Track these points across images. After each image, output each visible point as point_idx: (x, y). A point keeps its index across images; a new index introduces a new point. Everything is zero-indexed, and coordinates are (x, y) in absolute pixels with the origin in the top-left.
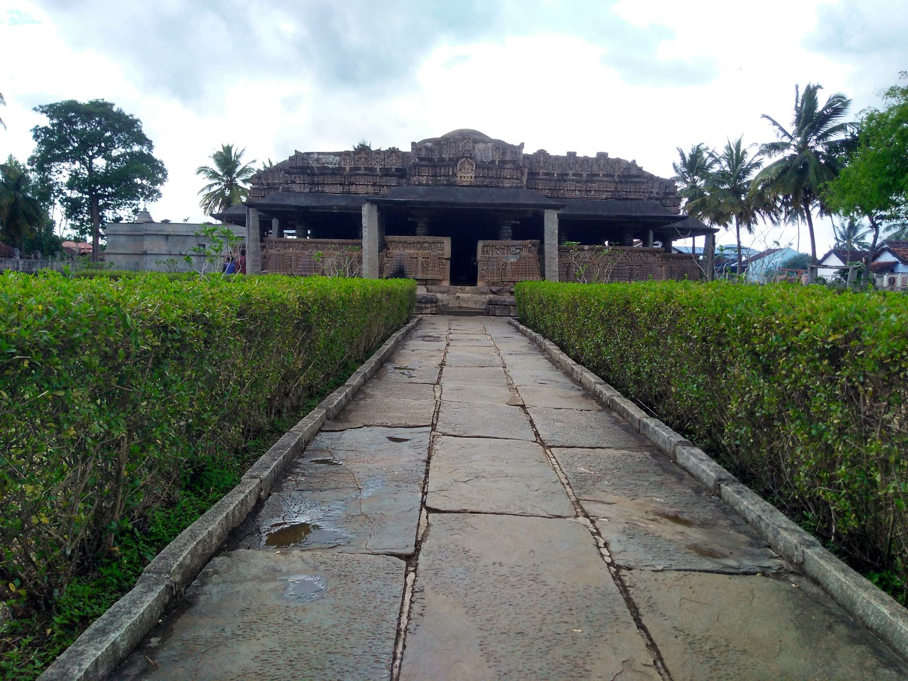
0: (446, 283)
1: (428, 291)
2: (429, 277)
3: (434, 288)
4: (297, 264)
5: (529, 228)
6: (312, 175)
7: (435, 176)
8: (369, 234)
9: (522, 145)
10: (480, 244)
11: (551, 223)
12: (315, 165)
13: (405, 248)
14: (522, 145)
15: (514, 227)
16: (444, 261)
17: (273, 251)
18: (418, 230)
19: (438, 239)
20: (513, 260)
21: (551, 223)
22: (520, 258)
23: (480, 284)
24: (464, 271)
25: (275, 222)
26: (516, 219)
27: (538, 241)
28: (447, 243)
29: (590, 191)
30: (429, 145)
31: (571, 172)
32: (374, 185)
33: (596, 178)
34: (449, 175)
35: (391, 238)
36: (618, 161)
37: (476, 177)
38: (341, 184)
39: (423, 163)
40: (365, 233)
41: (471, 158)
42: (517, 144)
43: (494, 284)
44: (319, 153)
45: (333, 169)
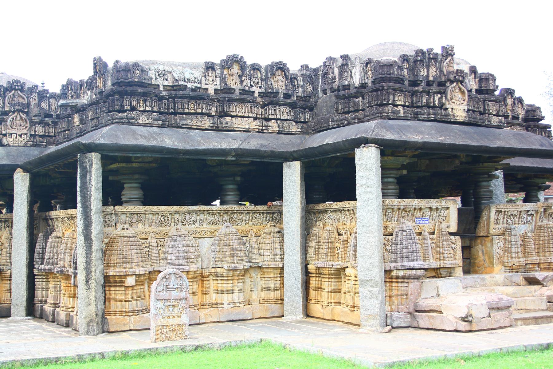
12: (161, 82)
34: (434, 107)
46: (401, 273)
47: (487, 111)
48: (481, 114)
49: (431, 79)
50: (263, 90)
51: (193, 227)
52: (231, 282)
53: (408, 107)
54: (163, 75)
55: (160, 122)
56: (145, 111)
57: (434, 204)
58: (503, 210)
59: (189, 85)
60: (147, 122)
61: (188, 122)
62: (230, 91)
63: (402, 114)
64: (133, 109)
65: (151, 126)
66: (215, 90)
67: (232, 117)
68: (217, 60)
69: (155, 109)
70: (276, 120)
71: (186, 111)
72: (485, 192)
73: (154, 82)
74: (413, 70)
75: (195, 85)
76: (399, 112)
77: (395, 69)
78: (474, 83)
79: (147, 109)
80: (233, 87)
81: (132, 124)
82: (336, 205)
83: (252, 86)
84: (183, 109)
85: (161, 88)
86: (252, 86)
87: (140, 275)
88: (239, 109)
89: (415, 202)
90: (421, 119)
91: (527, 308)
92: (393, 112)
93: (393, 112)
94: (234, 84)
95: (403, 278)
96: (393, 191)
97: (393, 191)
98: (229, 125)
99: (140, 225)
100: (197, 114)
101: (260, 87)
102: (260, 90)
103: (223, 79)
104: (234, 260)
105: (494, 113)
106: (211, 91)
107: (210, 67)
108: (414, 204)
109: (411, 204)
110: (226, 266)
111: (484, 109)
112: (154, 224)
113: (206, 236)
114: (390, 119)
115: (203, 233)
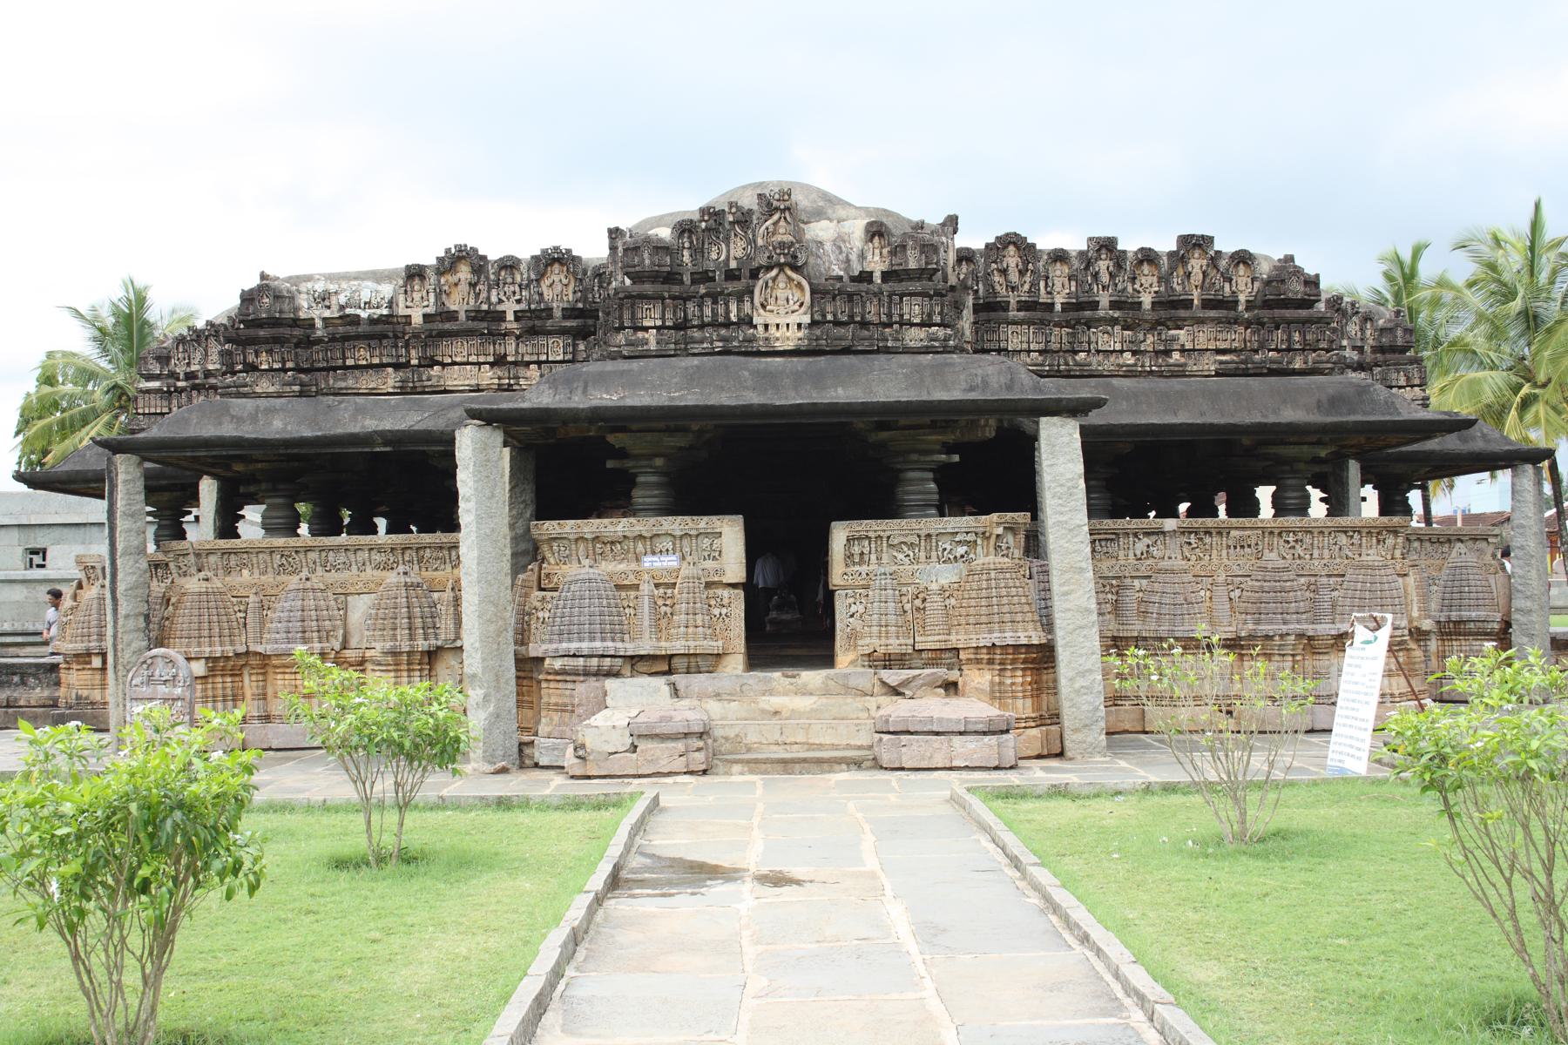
0: (736, 663)
1: (675, 692)
2: (678, 646)
3: (698, 681)
4: (262, 623)
5: (987, 471)
6: (308, 342)
7: (682, 326)
8: (479, 518)
9: (952, 223)
10: (840, 534)
11: (1060, 456)
12: (318, 314)
13: (597, 557)
14: (952, 223)
15: (943, 475)
17: (193, 584)
18: (639, 496)
19: (703, 522)
21: (1060, 456)
22: (971, 573)
23: (844, 658)
24: (788, 621)
25: (208, 489)
26: (949, 449)
27: (1022, 517)
29: (1167, 353)
30: (665, 233)
31: (1104, 299)
32: (499, 361)
33: (1182, 313)
34: (728, 324)
35: (551, 527)
36: (1243, 258)
37: (814, 324)
38: (397, 366)
39: (648, 288)
40: (467, 512)
41: (796, 269)
42: (934, 219)
43: (889, 661)
44: (330, 278)
45: (372, 321)
46: (558, 664)
47: (896, 318)
49: (733, 265)
50: (523, 306)
51: (345, 575)
53: (669, 328)
54: (324, 298)
55: (296, 388)
56: (271, 370)
57: (675, 526)
58: (871, 534)
59: (364, 314)
60: (272, 389)
61: (350, 383)
62: (451, 316)
63: (653, 346)
64: (251, 368)
65: (279, 395)
66: (425, 316)
67: (444, 365)
68: (429, 259)
69: (290, 365)
70: (539, 363)
71: (350, 362)
72: (908, 493)
73: (302, 315)
74: (698, 252)
75: (378, 312)
77: (646, 255)
78: (877, 258)
79: (276, 366)
80: (453, 308)
81: (245, 395)
82: (569, 526)
83: (501, 301)
84: (344, 358)
85: (319, 324)
86: (501, 301)
87: (215, 659)
88: (460, 350)
92: (630, 344)
93: (630, 344)
94: (458, 302)
95: (563, 672)
98: (434, 382)
99: (245, 572)
100: (371, 366)
101: (519, 301)
102: (518, 307)
103: (439, 293)
105: (917, 320)
106: (417, 319)
107: (415, 274)
108: (620, 528)
109: (611, 528)
110: (378, 646)
111: (890, 315)
114: (625, 358)
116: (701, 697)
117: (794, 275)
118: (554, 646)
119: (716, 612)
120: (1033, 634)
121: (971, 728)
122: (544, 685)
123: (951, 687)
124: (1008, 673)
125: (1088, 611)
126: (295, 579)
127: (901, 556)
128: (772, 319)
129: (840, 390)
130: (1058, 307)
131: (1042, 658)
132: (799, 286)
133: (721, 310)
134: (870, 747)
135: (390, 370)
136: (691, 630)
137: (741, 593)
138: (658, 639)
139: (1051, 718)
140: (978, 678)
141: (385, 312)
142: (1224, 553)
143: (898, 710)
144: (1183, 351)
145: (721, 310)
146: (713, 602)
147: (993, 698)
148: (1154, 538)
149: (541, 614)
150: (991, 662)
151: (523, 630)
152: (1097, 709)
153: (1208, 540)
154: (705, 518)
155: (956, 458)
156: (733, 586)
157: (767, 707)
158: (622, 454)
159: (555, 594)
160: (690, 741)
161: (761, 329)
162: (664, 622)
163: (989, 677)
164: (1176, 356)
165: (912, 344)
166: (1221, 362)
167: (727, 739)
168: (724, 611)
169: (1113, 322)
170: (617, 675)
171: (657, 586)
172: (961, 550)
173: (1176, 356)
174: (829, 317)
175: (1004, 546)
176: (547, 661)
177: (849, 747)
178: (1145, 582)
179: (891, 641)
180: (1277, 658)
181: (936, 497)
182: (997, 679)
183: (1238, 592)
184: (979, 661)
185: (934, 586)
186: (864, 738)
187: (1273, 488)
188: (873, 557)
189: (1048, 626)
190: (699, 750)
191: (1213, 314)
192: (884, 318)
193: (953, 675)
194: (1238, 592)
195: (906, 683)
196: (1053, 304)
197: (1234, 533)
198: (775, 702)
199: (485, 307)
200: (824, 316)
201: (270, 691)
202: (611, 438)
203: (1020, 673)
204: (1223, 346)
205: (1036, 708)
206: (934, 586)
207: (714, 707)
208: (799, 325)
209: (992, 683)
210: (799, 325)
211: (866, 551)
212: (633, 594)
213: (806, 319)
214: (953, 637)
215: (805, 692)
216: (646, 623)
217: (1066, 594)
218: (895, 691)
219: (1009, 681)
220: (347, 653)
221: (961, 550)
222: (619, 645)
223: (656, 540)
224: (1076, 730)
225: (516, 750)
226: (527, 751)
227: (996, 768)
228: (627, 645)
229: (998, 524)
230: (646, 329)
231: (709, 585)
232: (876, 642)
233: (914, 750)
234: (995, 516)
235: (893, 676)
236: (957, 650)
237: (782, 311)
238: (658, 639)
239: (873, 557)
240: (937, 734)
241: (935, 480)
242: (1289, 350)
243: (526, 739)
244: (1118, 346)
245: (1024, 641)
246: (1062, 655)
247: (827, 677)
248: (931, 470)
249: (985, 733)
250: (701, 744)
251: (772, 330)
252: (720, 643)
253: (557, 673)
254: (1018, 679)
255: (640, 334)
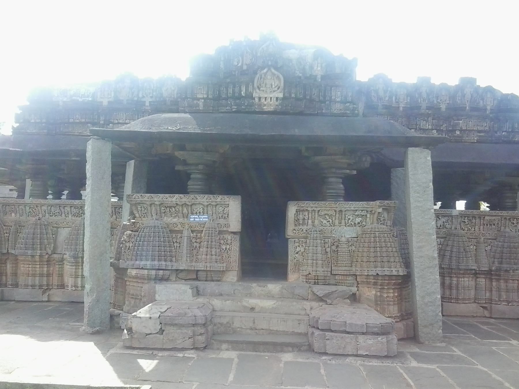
0: (232, 276)
2: (201, 266)
3: (210, 287)
5: (372, 178)
15: (347, 180)
16: (229, 237)
18: (191, 185)
19: (219, 198)
20: (348, 233)
21: (419, 171)
22: (364, 233)
23: (292, 277)
28: (233, 208)
29: (454, 131)
36: (490, 90)
37: (284, 98)
46: (134, 272)
48: (322, 102)
50: (154, 99)
52: (74, 268)
57: (204, 200)
58: (309, 209)
72: (329, 189)
75: (87, 99)
76: (198, 105)
89: (175, 198)
90: (223, 111)
91: (271, 328)
95: (136, 277)
96: (199, 187)
97: (199, 187)
99: (13, 215)
102: (151, 100)
104: (76, 249)
108: (174, 199)
111: (325, 97)
112: (24, 214)
113: (67, 226)
115: (65, 223)
116: (213, 295)
117: (276, 72)
118: (133, 262)
119: (224, 247)
120: (400, 269)
121: (370, 330)
122: (128, 283)
123: (354, 298)
124: (385, 291)
125: (434, 258)
126: (34, 219)
127: (325, 222)
128: (263, 95)
129: (296, 130)
130: (401, 109)
131: (405, 282)
132: (278, 77)
133: (237, 90)
134: (306, 334)
135: (89, 125)
136: (208, 257)
137: (238, 237)
138: (191, 261)
139: (408, 315)
140: (369, 293)
141: (90, 99)
142: (482, 227)
143: (325, 313)
144: (461, 130)
145: (237, 90)
146: (222, 242)
147: (377, 304)
148: (446, 218)
149: (128, 245)
150: (375, 284)
151: (120, 253)
152: (437, 315)
153: (474, 221)
154: (220, 196)
155: (355, 172)
156: (234, 233)
157: (246, 305)
158: (185, 163)
159: (137, 233)
160: (196, 328)
161: (257, 100)
162: (195, 252)
163: (374, 292)
164: (458, 133)
165: (335, 112)
166: (480, 136)
167: (221, 324)
168: (228, 247)
169: (429, 115)
170: (167, 280)
171: (193, 232)
172: (358, 220)
173: (458, 133)
174: (293, 95)
175: (382, 219)
176: (129, 271)
177: (294, 334)
178: (442, 240)
179: (318, 269)
180: (511, 281)
181: (343, 192)
182: (379, 294)
183: (489, 247)
184: (368, 283)
185: (343, 239)
186: (302, 329)
187: (465, 201)
188: (310, 221)
189: (407, 263)
190: (201, 334)
191: (476, 113)
192: (321, 98)
193: (354, 289)
194: (489, 247)
195: (328, 295)
196: (399, 107)
197: (487, 218)
198: (252, 302)
199: (136, 99)
200: (290, 95)
201: (19, 272)
202: (177, 153)
203: (392, 291)
204: (480, 128)
205: (400, 310)
206: (343, 239)
207: (217, 303)
208: (277, 98)
209: (376, 295)
210: (277, 98)
211: (306, 218)
212: (179, 235)
213: (281, 95)
214: (354, 269)
215: (270, 296)
216: (185, 252)
217: (420, 247)
218: (321, 299)
219: (385, 295)
220: (55, 256)
221: (358, 220)
222: (169, 263)
223: (194, 207)
224: (425, 326)
225: (108, 319)
226: (116, 319)
227: (386, 357)
228: (174, 264)
229: (380, 207)
230: (199, 99)
231: (220, 232)
232: (310, 269)
233: (334, 342)
234: (378, 202)
235: (320, 290)
236: (356, 275)
237: (268, 91)
238: (191, 261)
239: (310, 221)
240: (348, 333)
241: (343, 183)
242: (512, 131)
243: (117, 312)
244: (430, 127)
245: (395, 273)
246: (418, 281)
247: (282, 288)
248: (341, 178)
249: (377, 334)
250: (203, 331)
251: (263, 100)
252: (225, 265)
253: (133, 277)
254: (391, 294)
255: (195, 102)
